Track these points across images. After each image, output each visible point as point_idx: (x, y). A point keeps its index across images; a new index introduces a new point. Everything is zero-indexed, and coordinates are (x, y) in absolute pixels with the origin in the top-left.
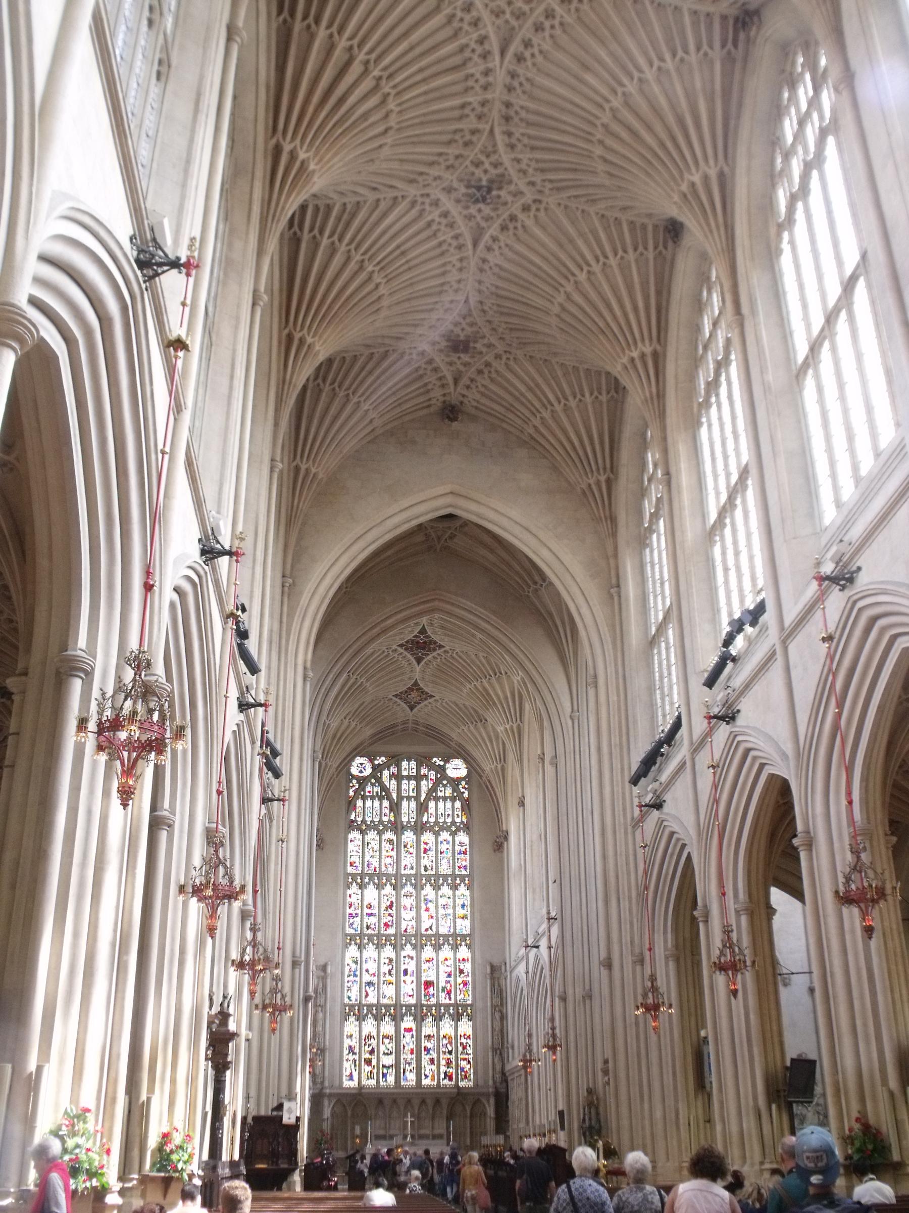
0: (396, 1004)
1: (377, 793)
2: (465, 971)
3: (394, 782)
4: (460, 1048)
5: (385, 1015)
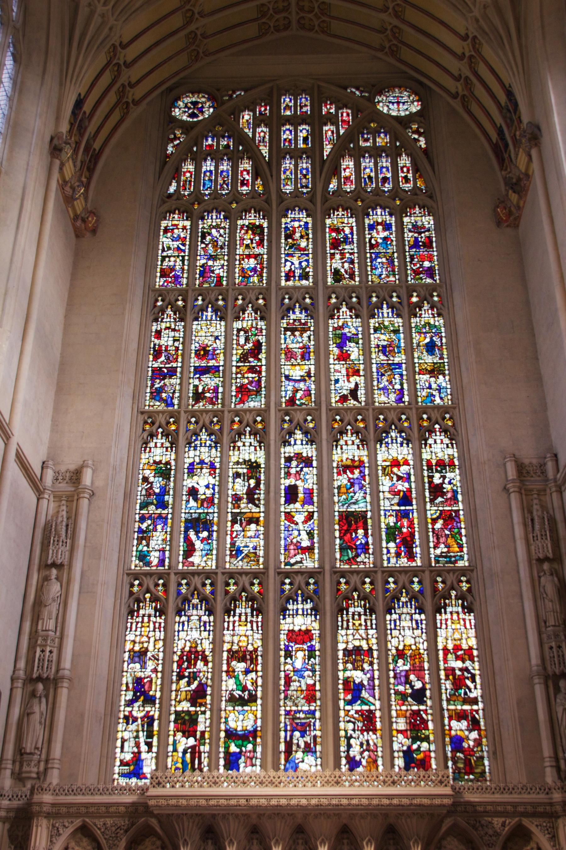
0: (266, 568)
1: (228, 146)
2: (447, 487)
3: (263, 131)
4: (448, 685)
5: (235, 599)
